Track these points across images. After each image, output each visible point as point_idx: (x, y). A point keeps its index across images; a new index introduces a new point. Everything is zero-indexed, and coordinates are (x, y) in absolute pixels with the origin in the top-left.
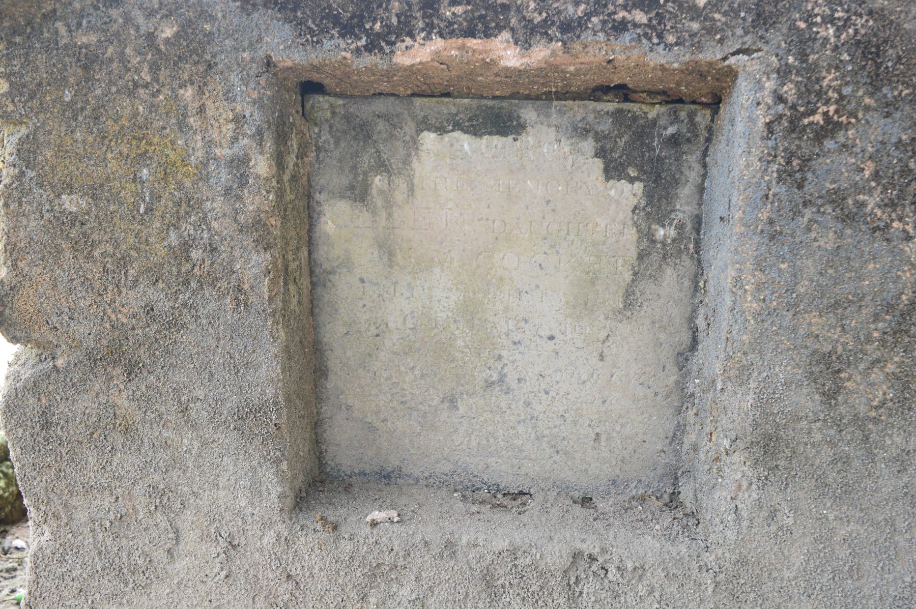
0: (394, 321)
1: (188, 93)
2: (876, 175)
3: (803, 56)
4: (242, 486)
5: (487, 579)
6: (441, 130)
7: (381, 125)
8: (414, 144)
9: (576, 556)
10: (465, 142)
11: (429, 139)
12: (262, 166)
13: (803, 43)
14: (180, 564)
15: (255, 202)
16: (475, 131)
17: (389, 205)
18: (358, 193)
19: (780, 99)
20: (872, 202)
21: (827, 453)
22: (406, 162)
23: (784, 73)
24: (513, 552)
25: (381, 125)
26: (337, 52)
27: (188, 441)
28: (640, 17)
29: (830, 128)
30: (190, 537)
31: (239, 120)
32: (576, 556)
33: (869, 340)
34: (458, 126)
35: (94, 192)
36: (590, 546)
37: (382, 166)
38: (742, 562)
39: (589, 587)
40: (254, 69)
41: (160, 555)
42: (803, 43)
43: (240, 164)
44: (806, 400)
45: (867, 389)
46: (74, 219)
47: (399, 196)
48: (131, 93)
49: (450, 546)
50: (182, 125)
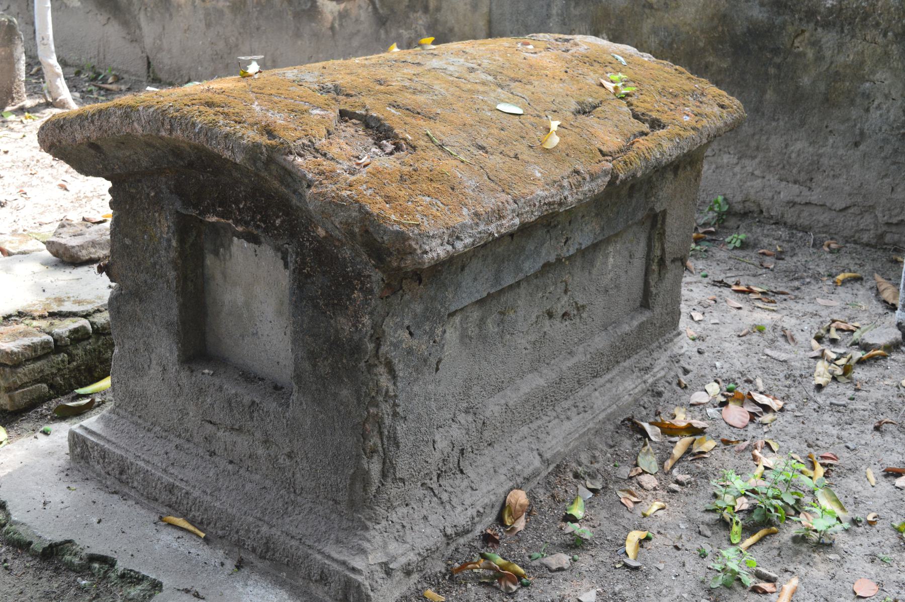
0: (226, 303)
1: (157, 215)
2: (321, 294)
3: (302, 250)
6: (239, 238)
7: (222, 231)
8: (231, 241)
11: (235, 239)
12: (174, 243)
13: (301, 245)
14: (152, 371)
15: (173, 254)
16: (248, 241)
17: (225, 259)
19: (296, 262)
20: (321, 303)
21: (314, 387)
23: (297, 254)
24: (236, 394)
25: (222, 231)
26: (194, 212)
28: (263, 226)
29: (308, 276)
30: (154, 362)
31: (169, 227)
33: (322, 350)
34: (243, 238)
35: (133, 239)
37: (222, 246)
38: (294, 418)
39: (255, 414)
40: (173, 212)
41: (146, 366)
42: (301, 245)
43: (169, 240)
44: (307, 365)
45: (324, 367)
46: (128, 246)
47: (227, 257)
48: (143, 210)
50: (155, 224)
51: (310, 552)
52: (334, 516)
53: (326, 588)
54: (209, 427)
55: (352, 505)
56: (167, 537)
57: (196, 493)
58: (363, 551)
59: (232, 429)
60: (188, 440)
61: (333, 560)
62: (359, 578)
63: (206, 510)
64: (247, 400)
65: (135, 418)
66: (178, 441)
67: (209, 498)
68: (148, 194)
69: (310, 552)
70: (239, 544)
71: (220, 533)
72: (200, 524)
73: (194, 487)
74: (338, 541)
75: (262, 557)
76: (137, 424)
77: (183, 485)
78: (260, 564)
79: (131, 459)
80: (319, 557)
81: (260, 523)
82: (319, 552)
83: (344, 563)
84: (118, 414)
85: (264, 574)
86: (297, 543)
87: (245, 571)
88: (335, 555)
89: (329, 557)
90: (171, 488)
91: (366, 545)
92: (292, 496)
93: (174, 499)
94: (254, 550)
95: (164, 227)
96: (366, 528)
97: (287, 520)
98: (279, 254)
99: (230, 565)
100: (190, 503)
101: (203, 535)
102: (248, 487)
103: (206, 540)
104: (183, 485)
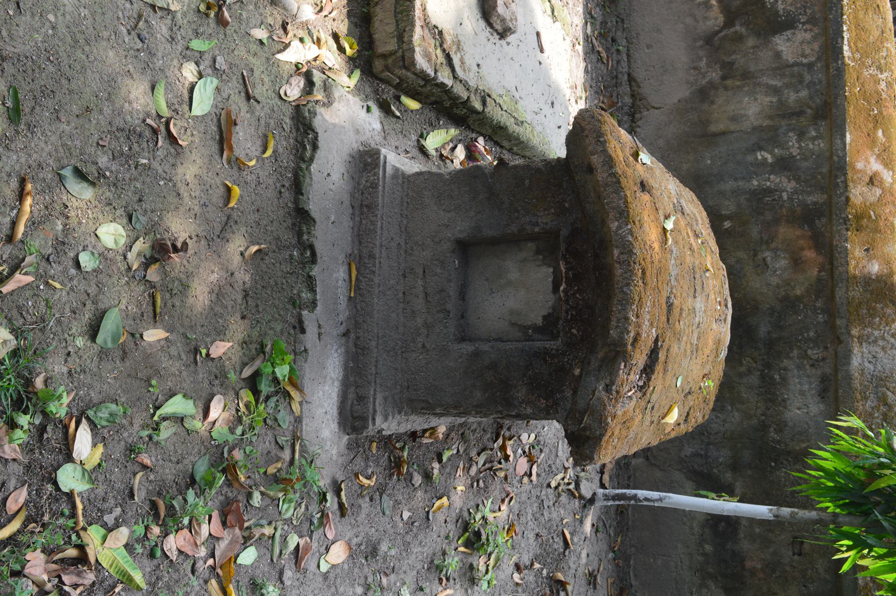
4: (462, 227)
5: (443, 290)
6: (553, 273)
8: (550, 266)
9: (449, 312)
10: (550, 279)
11: (551, 270)
12: (537, 230)
16: (553, 282)
18: (538, 252)
22: (546, 264)
24: (449, 296)
27: (473, 214)
31: (547, 224)
32: (449, 312)
36: (451, 315)
38: (449, 351)
39: (442, 315)
43: (537, 224)
49: (450, 281)
51: (373, 384)
52: (398, 387)
53: (355, 402)
54: (420, 271)
55: (410, 401)
56: (341, 273)
57: (376, 280)
58: (386, 419)
59: (426, 293)
60: (406, 251)
61: (374, 402)
62: (371, 427)
63: (369, 291)
64: (449, 307)
65: (405, 199)
66: (402, 244)
67: (377, 291)
68: (565, 201)
69: (373, 384)
70: (357, 325)
71: (359, 307)
72: (358, 288)
73: (379, 275)
74: (385, 398)
75: (356, 345)
76: (402, 202)
77: (378, 266)
78: (351, 344)
79: (379, 213)
80: (372, 392)
81: (376, 338)
82: (375, 390)
83: (375, 411)
84: (403, 182)
85: (347, 352)
86: (374, 372)
87: (343, 340)
88: (377, 404)
89: (375, 399)
90: (372, 256)
91: (390, 418)
92: (399, 352)
93: (366, 261)
94: (358, 338)
95: (545, 219)
96: (400, 413)
97: (384, 356)
98: (551, 311)
99: (342, 329)
100: (368, 276)
101: (352, 295)
102: (394, 315)
103: (350, 297)
104: (378, 266)
